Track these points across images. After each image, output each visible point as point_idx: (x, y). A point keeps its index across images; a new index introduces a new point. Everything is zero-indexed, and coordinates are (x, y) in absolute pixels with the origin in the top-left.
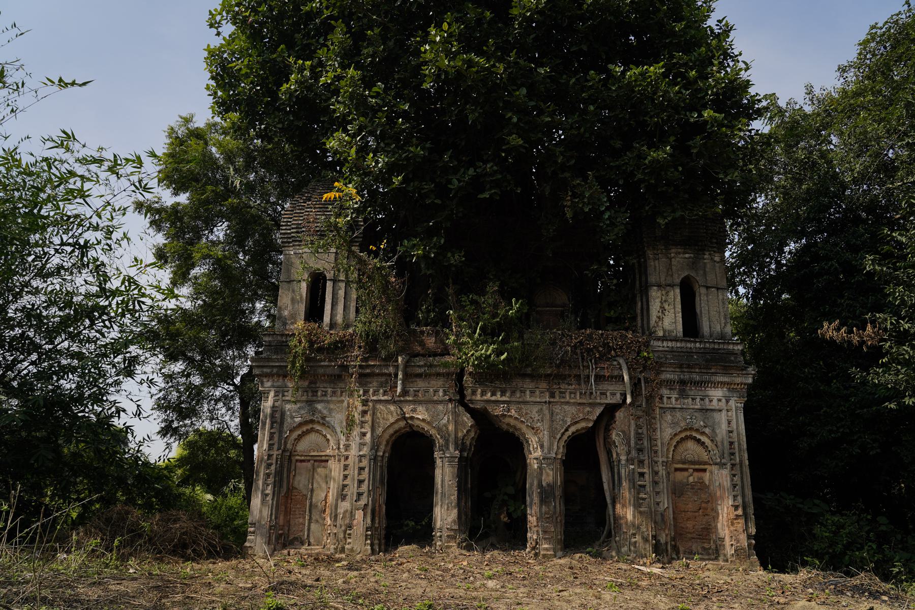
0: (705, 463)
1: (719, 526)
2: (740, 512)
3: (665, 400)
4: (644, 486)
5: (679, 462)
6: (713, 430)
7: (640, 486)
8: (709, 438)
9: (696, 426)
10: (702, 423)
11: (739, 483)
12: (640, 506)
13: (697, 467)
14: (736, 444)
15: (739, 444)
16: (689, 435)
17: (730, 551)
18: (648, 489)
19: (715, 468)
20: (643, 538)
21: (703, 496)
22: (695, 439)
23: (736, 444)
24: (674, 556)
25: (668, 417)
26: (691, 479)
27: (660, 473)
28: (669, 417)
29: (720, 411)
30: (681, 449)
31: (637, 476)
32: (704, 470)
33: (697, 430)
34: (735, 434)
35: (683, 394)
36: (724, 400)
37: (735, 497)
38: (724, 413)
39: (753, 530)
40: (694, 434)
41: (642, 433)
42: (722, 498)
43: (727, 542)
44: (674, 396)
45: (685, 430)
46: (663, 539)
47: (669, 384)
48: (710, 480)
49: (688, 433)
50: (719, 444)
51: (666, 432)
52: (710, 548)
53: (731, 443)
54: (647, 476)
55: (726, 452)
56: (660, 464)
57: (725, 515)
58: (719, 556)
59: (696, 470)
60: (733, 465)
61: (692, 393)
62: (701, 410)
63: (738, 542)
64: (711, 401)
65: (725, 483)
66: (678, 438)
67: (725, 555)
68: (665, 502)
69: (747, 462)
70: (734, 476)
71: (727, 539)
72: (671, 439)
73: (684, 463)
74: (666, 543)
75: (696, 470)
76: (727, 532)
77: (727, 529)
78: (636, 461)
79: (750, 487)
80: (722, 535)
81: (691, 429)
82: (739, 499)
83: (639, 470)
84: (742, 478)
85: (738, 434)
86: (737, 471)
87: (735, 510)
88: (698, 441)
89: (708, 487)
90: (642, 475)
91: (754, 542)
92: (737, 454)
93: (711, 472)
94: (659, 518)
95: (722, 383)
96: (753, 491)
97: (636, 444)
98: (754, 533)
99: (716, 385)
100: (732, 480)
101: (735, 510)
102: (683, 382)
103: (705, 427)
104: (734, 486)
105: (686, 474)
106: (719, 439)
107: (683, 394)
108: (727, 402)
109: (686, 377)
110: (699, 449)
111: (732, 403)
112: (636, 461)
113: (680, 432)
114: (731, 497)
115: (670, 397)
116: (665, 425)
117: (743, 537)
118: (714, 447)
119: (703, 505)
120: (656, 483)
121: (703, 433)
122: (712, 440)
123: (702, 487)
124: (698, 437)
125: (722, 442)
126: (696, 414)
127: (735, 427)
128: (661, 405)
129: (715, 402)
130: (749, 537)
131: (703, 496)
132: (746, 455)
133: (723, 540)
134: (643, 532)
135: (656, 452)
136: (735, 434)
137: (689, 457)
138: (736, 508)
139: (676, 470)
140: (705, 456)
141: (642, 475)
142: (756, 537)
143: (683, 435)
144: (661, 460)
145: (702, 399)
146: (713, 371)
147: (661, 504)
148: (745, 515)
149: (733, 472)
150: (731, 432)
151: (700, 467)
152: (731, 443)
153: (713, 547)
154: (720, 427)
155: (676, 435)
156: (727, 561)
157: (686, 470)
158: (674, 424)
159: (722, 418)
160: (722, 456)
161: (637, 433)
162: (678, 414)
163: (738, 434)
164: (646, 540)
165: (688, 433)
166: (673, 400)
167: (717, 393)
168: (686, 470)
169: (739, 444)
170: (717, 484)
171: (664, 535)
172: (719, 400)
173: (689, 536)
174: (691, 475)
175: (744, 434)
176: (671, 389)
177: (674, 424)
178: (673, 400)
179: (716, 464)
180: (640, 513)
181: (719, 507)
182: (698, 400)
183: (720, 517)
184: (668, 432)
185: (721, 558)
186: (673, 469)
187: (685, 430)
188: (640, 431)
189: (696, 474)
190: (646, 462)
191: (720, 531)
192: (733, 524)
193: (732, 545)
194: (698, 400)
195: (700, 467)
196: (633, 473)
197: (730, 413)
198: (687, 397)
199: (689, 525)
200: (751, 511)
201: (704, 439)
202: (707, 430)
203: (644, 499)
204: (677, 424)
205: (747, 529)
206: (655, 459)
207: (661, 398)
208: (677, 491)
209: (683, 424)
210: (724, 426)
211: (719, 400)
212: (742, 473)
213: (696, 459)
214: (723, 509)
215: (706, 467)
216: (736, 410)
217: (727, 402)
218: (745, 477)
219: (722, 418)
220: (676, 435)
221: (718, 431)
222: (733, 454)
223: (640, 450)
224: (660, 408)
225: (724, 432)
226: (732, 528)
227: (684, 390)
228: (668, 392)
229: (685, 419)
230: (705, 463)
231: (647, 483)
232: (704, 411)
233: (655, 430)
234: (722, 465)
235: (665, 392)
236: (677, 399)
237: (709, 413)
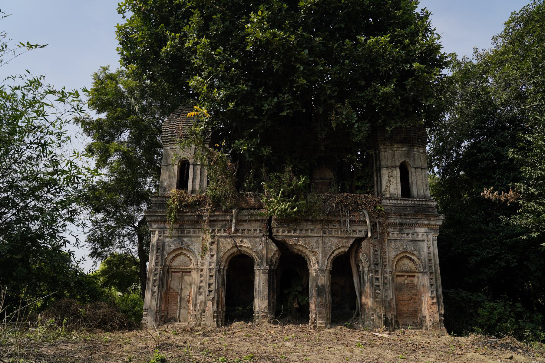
0: (415, 272)
1: (423, 309)
2: (435, 301)
3: (391, 235)
4: (379, 286)
7: (376, 286)
8: (417, 257)
9: (409, 250)
10: (412, 248)
11: (435, 283)
12: (376, 297)
13: (410, 274)
14: (433, 261)
15: (435, 261)
16: (405, 255)
17: (429, 324)
18: (381, 287)
19: (420, 275)
20: (378, 316)
21: (413, 291)
22: (408, 258)
23: (433, 261)
24: (396, 327)
25: (393, 245)
26: (406, 282)
27: (388, 278)
28: (393, 245)
29: (423, 241)
30: (400, 263)
31: (374, 280)
32: (414, 276)
33: (410, 253)
34: (432, 255)
35: (401, 232)
36: (425, 235)
37: (432, 292)
38: (426, 242)
39: (443, 312)
40: (408, 255)
41: (377, 255)
42: (424, 293)
43: (428, 318)
44: (396, 232)
45: (403, 252)
46: (390, 317)
47: (393, 225)
48: (417, 282)
49: (405, 254)
51: (391, 253)
52: (417, 322)
53: (430, 260)
54: (380, 280)
55: (427, 265)
56: (388, 272)
57: (426, 303)
58: (422, 327)
60: (431, 273)
61: (407, 230)
62: (412, 241)
63: (434, 318)
64: (418, 235)
65: (426, 284)
66: (398, 257)
67: (426, 326)
68: (391, 295)
69: (439, 271)
70: (432, 279)
71: (428, 317)
73: (402, 272)
74: (392, 319)
76: (427, 312)
77: (427, 310)
78: (374, 271)
79: (441, 286)
80: (424, 314)
81: (406, 252)
82: (435, 293)
83: (376, 276)
84: (436, 281)
85: (434, 255)
86: (433, 276)
87: (432, 300)
88: (411, 259)
89: (416, 286)
90: (377, 279)
91: (443, 318)
92: (433, 267)
93: (418, 277)
94: (387, 305)
95: (424, 224)
96: (442, 288)
97: (374, 261)
98: (443, 313)
99: (421, 226)
100: (430, 282)
101: (432, 300)
102: (401, 224)
104: (432, 285)
105: (403, 278)
106: (422, 257)
107: (401, 232)
108: (428, 235)
109: (403, 221)
111: (430, 236)
112: (374, 271)
113: (400, 254)
114: (430, 292)
115: (394, 233)
116: (391, 249)
117: (437, 316)
118: (420, 263)
119: (413, 297)
120: (385, 284)
121: (413, 254)
123: (412, 286)
124: (410, 256)
125: (425, 260)
126: (409, 243)
127: (432, 251)
128: (388, 238)
129: (420, 236)
130: (440, 315)
131: (413, 291)
132: (439, 267)
133: (425, 317)
134: (378, 313)
135: (385, 266)
136: (432, 255)
137: (405, 269)
138: (433, 298)
139: (398, 276)
140: (414, 268)
141: (377, 279)
142: (444, 316)
143: (401, 255)
144: (388, 270)
145: (412, 234)
146: (419, 217)
147: (388, 296)
148: (438, 302)
149: (431, 277)
150: (430, 253)
151: (411, 274)
152: (430, 260)
153: (419, 321)
154: (423, 251)
155: (397, 255)
156: (427, 329)
158: (396, 249)
159: (425, 245)
161: (374, 255)
162: (399, 243)
163: (434, 255)
164: (379, 318)
165: (405, 254)
166: (396, 235)
167: (421, 231)
169: (435, 261)
170: (422, 284)
171: (390, 315)
172: (423, 235)
173: (405, 315)
174: (406, 279)
175: (437, 255)
176: (394, 228)
177: (396, 249)
178: (396, 235)
179: (421, 272)
180: (376, 301)
181: (423, 298)
182: (410, 235)
183: (424, 304)
184: (393, 254)
185: (424, 328)
187: (403, 252)
188: (376, 253)
189: (409, 278)
190: (380, 272)
191: (423, 312)
192: (431, 308)
193: (430, 320)
194: (410, 235)
195: (411, 274)
196: (372, 278)
197: (429, 243)
198: (404, 233)
199: (405, 308)
200: (441, 300)
201: (414, 258)
202: (416, 253)
203: (378, 293)
205: (439, 311)
206: (385, 270)
207: (389, 234)
208: (398, 288)
209: (401, 249)
210: (426, 250)
211: (423, 235)
212: (436, 278)
213: (409, 269)
214: (425, 300)
215: (415, 274)
216: (433, 241)
217: (428, 235)
218: (438, 280)
219: (425, 245)
220: (397, 255)
221: (422, 253)
222: (431, 266)
223: (376, 265)
224: (388, 239)
225: (426, 254)
226: (430, 310)
227: (402, 229)
228: (393, 230)
229: (403, 246)
230: (415, 272)
231: (380, 284)
232: (414, 241)
234: (424, 273)
235: (391, 230)
236: (398, 234)
237: (417, 243)
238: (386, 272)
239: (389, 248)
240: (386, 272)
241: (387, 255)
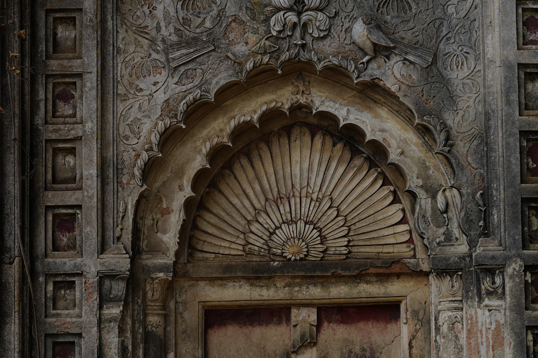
0: (391, 269)
5: (228, 273)
6: (433, 71)
10: (359, 30)
13: (340, 292)
19: (438, 293)
30: (244, 193)
32: (388, 311)
33: (335, 76)
40: (322, 101)
45: (260, 78)
49: (284, 97)
50: (462, 148)
55: (500, 194)
56: (85, 295)
59: (330, 312)
66: (219, 129)
72: (170, 138)
73: (258, 272)
75: (330, 312)
81: (298, 71)
88: (350, 139)
93: (423, 319)
103: (379, 51)
106: (462, 119)
110: (358, 188)
113: (229, 93)
116: (132, 51)
118: (439, 173)
121: (372, 92)
122: (424, 131)
124: (346, 113)
125: (484, 139)
135: (66, 221)
139: (217, 316)
140: (387, 229)
143: (251, 109)
144: (92, 265)
154: (474, 48)
155: (199, 112)
157: (278, 313)
160: (480, 224)
165: (284, 97)
168: (278, 313)
177: (195, 45)
179: (444, 270)
184: (151, 98)
186: (192, 317)
187: (260, 78)
201: (379, 125)
202: (393, 73)
204: (213, 42)
206: (65, 262)
209: (246, 44)
213: (337, 245)
215: (394, 289)
220: (199, 112)
221: (457, 75)
225: (496, 77)
229: (261, 13)
230: (391, 269)
233: (65, 89)
234: (475, 276)
238: (66, 282)
239: (123, 37)
240: (66, 282)
241: (87, 105)
